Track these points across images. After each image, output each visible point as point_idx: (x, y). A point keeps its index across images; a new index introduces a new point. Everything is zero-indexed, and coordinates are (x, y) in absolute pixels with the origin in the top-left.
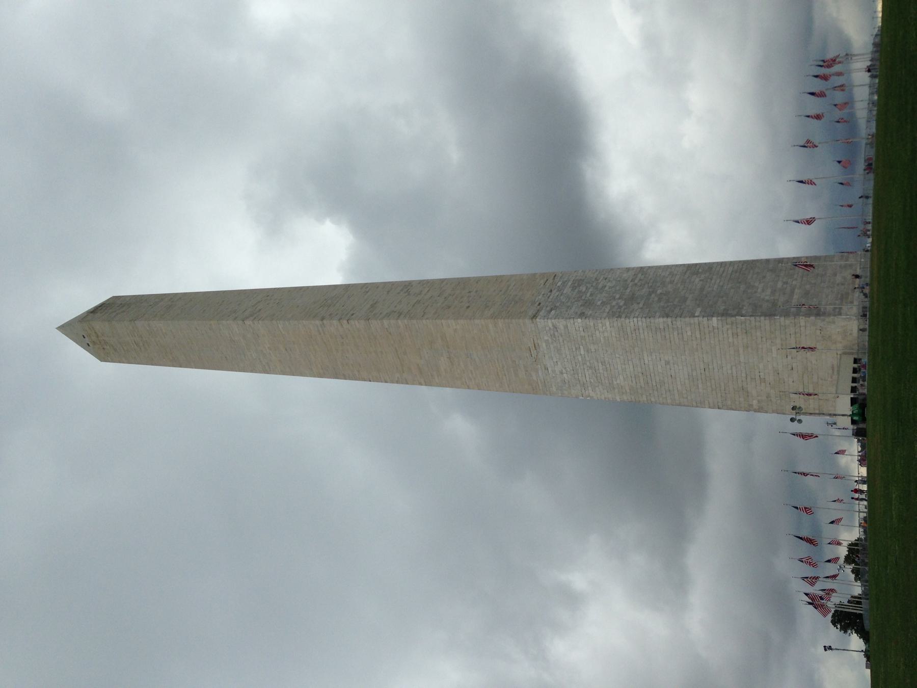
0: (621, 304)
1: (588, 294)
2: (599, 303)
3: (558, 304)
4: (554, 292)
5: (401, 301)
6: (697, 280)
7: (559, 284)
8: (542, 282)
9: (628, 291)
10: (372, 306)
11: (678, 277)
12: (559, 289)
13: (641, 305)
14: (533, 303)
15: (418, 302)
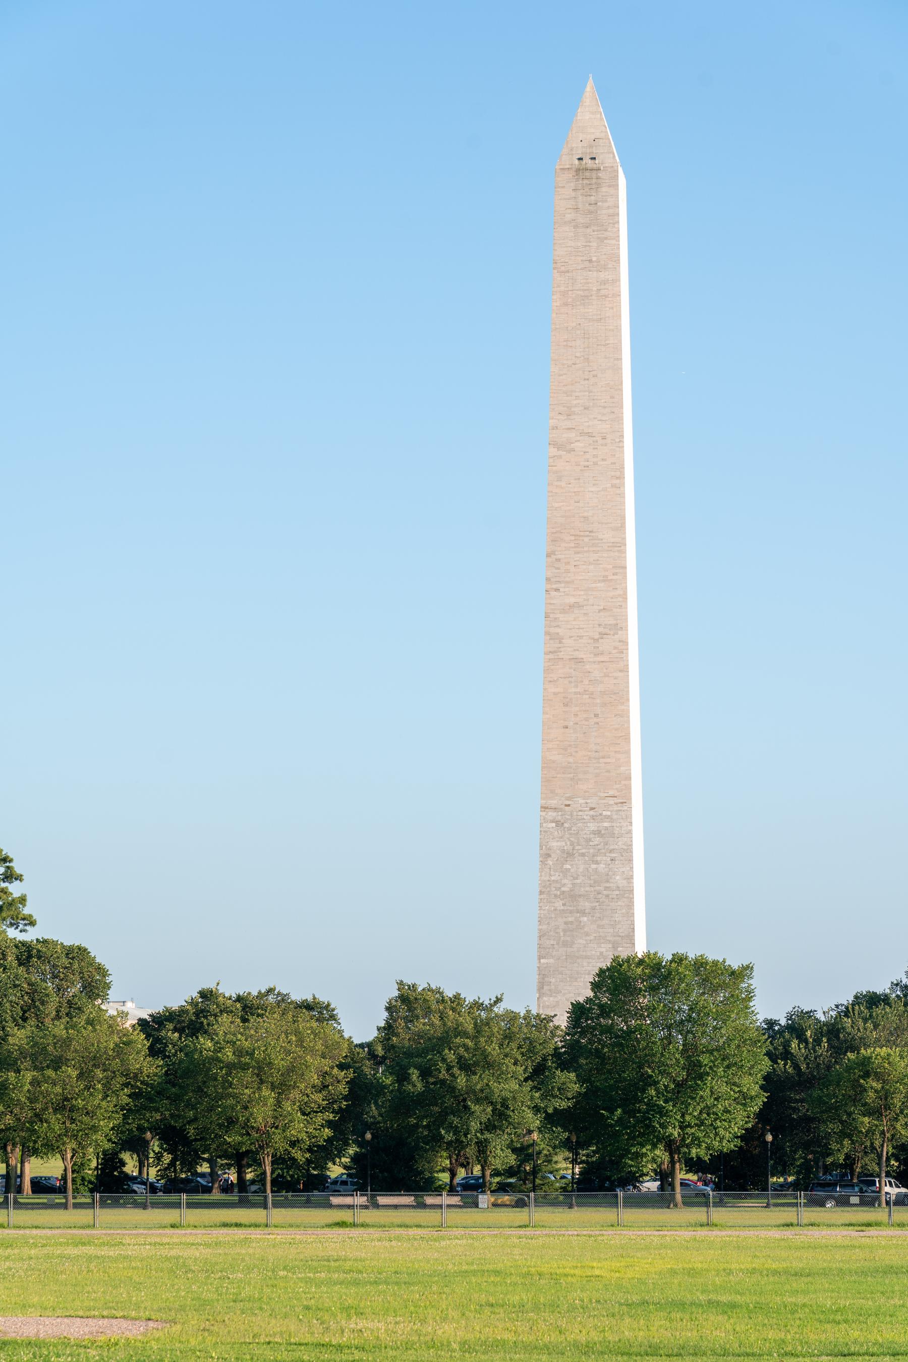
0: (563, 889)
1: (584, 851)
2: (568, 866)
3: (566, 825)
4: (592, 813)
5: (581, 637)
6: (604, 950)
7: (604, 813)
8: (611, 793)
9: (588, 889)
10: (571, 606)
11: (611, 930)
12: (593, 817)
13: (562, 908)
14: (569, 799)
15: (579, 661)
